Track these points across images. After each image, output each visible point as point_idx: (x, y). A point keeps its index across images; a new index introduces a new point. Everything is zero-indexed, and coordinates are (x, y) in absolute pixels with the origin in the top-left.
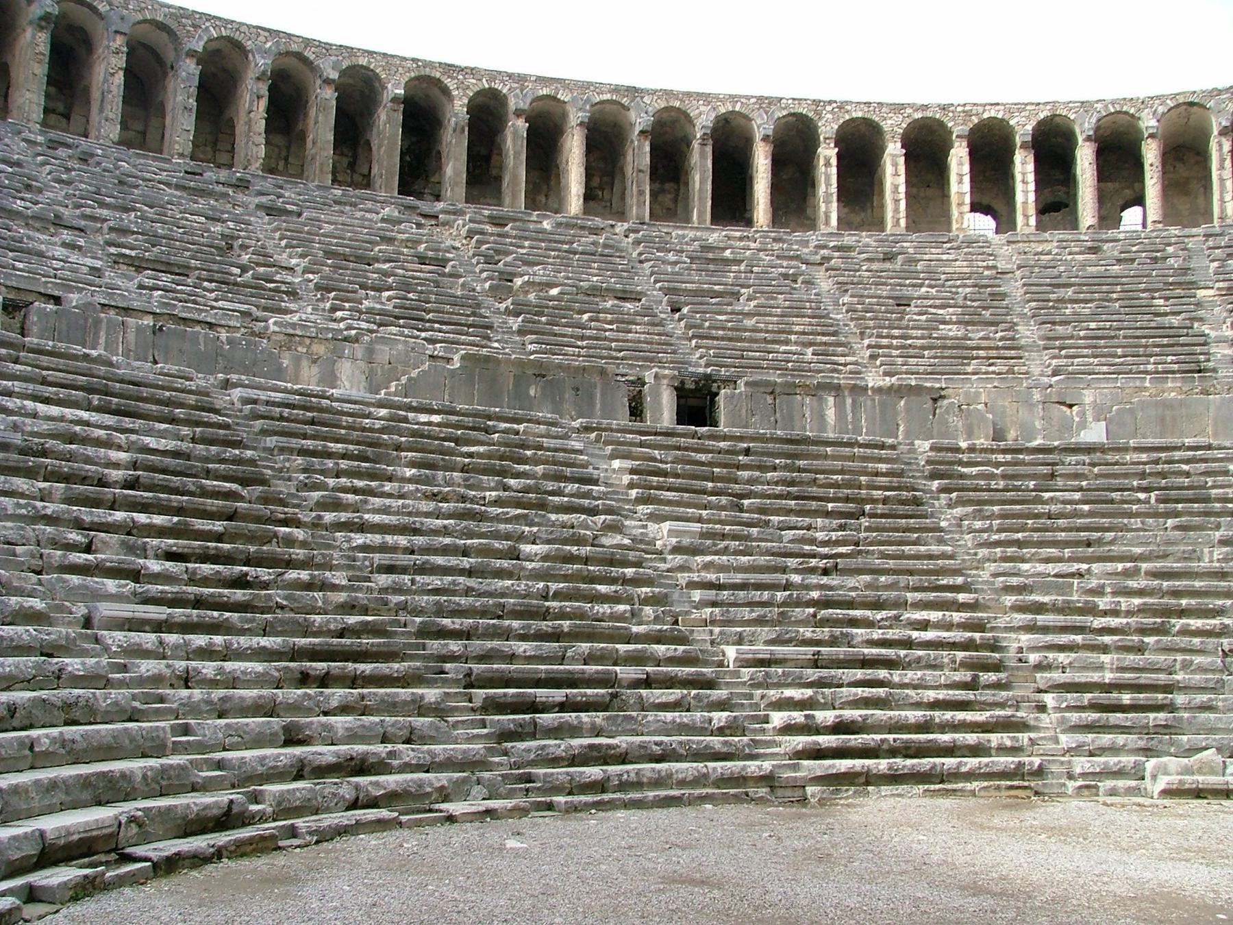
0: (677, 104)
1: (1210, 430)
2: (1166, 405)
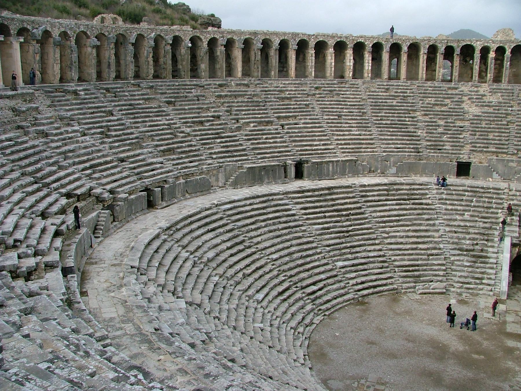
0: (268, 37)
2: (410, 163)
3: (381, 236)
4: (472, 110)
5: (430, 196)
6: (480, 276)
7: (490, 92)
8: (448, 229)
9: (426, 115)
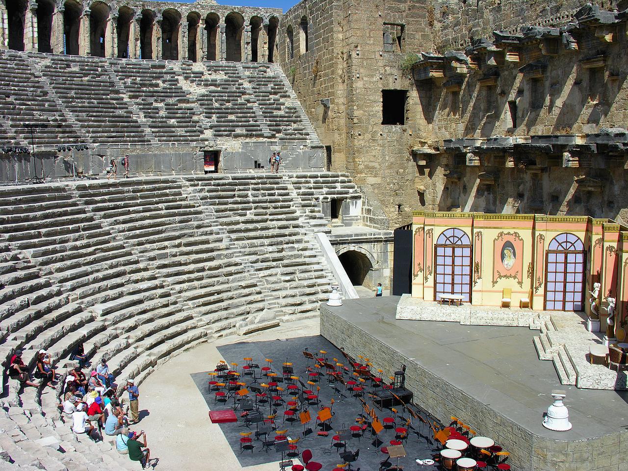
1: (153, 166)
3: (142, 256)
4: (195, 90)
5: (186, 195)
6: (312, 290)
7: (209, 70)
8: (234, 236)
9: (136, 97)
